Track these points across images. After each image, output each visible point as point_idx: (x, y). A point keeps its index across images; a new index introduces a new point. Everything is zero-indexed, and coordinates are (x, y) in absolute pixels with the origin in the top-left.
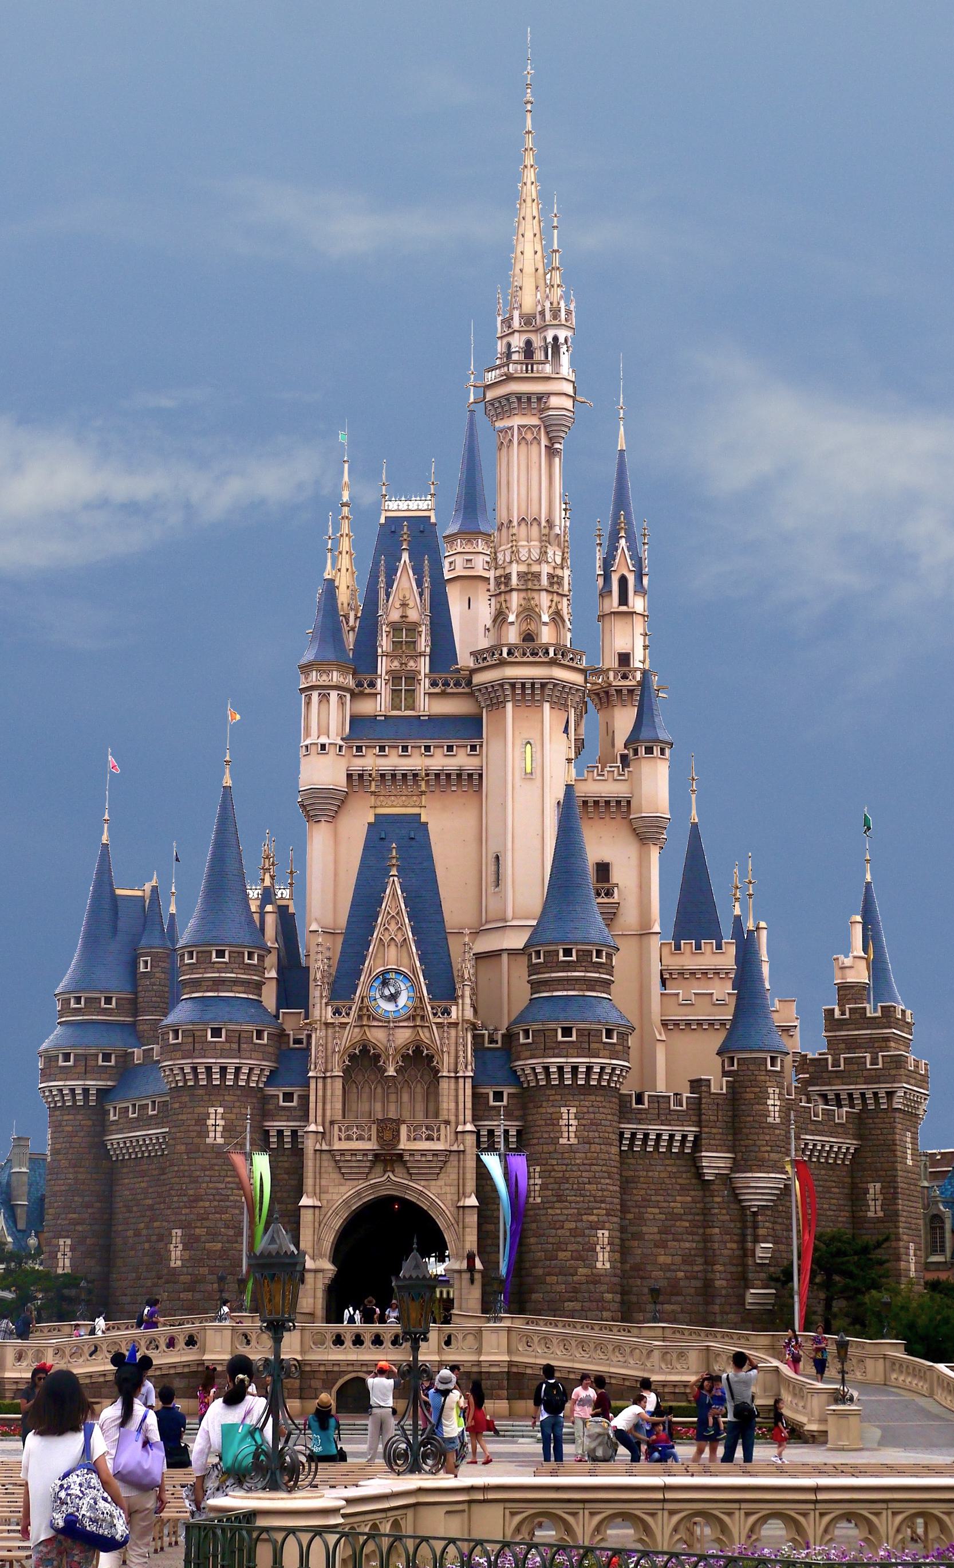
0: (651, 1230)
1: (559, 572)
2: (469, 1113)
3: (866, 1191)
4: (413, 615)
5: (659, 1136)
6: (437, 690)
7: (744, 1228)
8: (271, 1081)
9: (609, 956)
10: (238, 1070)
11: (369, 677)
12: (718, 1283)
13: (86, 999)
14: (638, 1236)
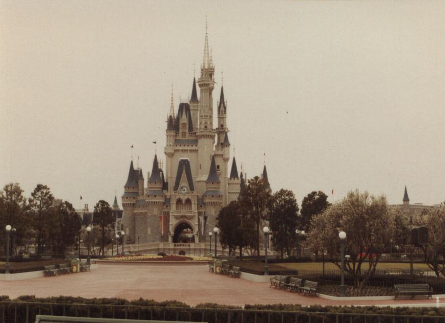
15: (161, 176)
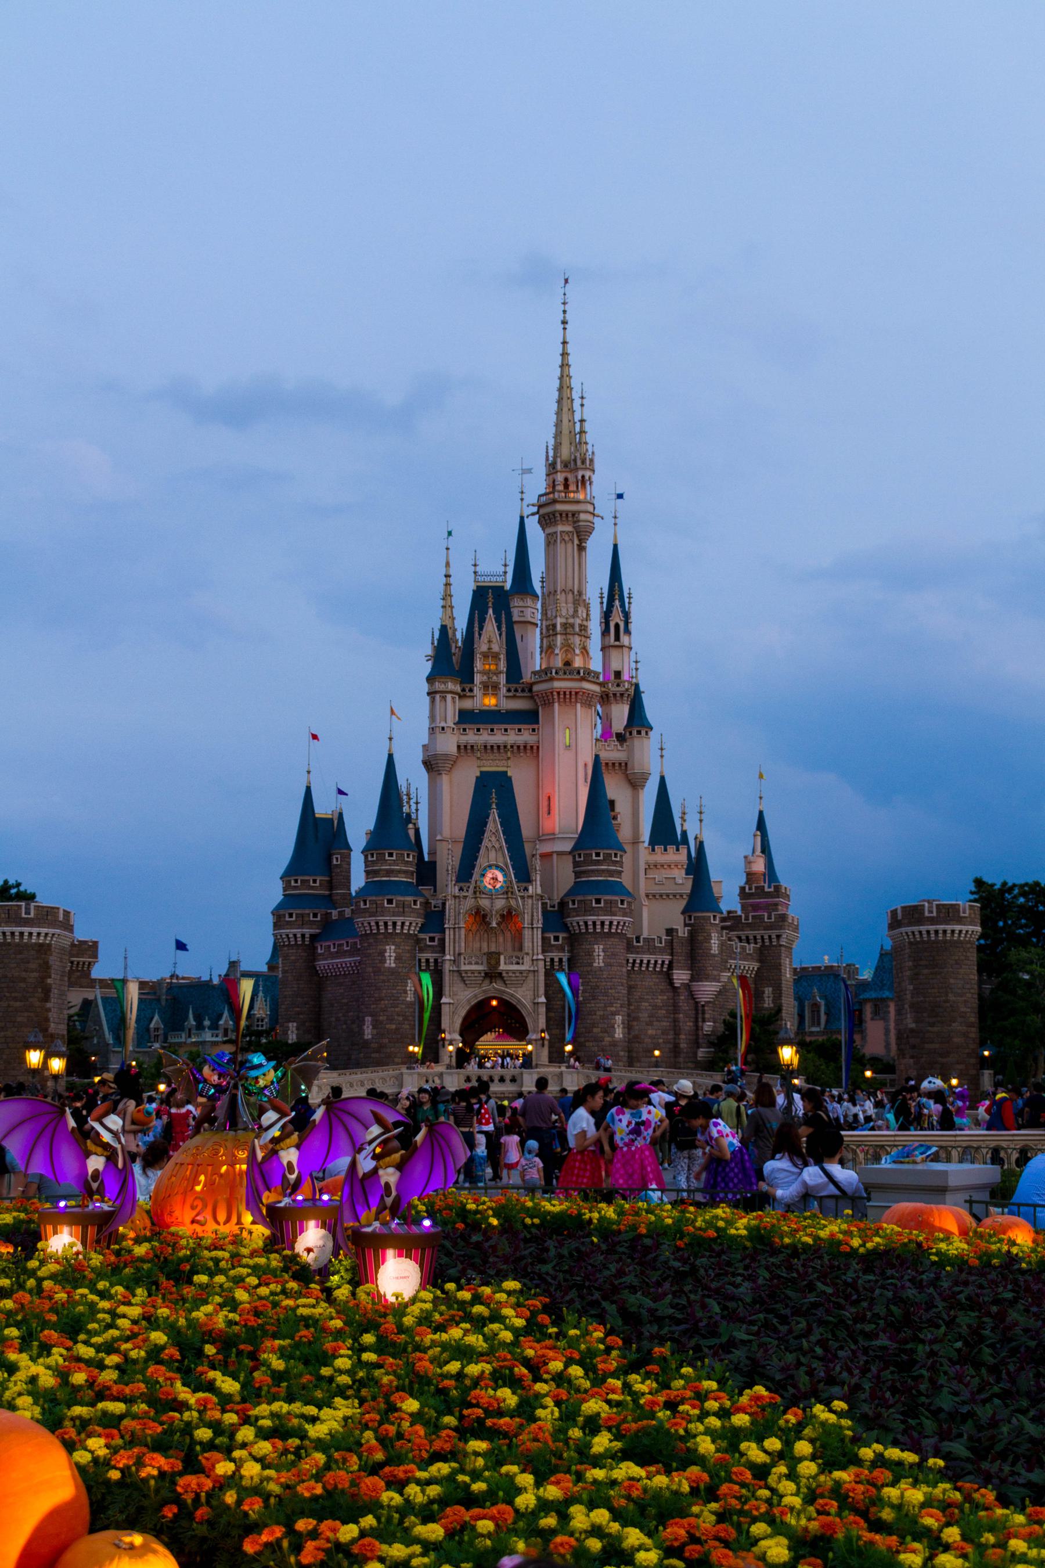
0: (644, 1016)
1: (585, 623)
2: (540, 949)
3: (763, 992)
4: (496, 648)
5: (649, 961)
6: (511, 694)
7: (697, 1014)
8: (421, 931)
9: (621, 856)
10: (403, 924)
11: (469, 686)
12: (682, 1046)
13: (302, 881)
14: (636, 1019)
15: (412, 833)
